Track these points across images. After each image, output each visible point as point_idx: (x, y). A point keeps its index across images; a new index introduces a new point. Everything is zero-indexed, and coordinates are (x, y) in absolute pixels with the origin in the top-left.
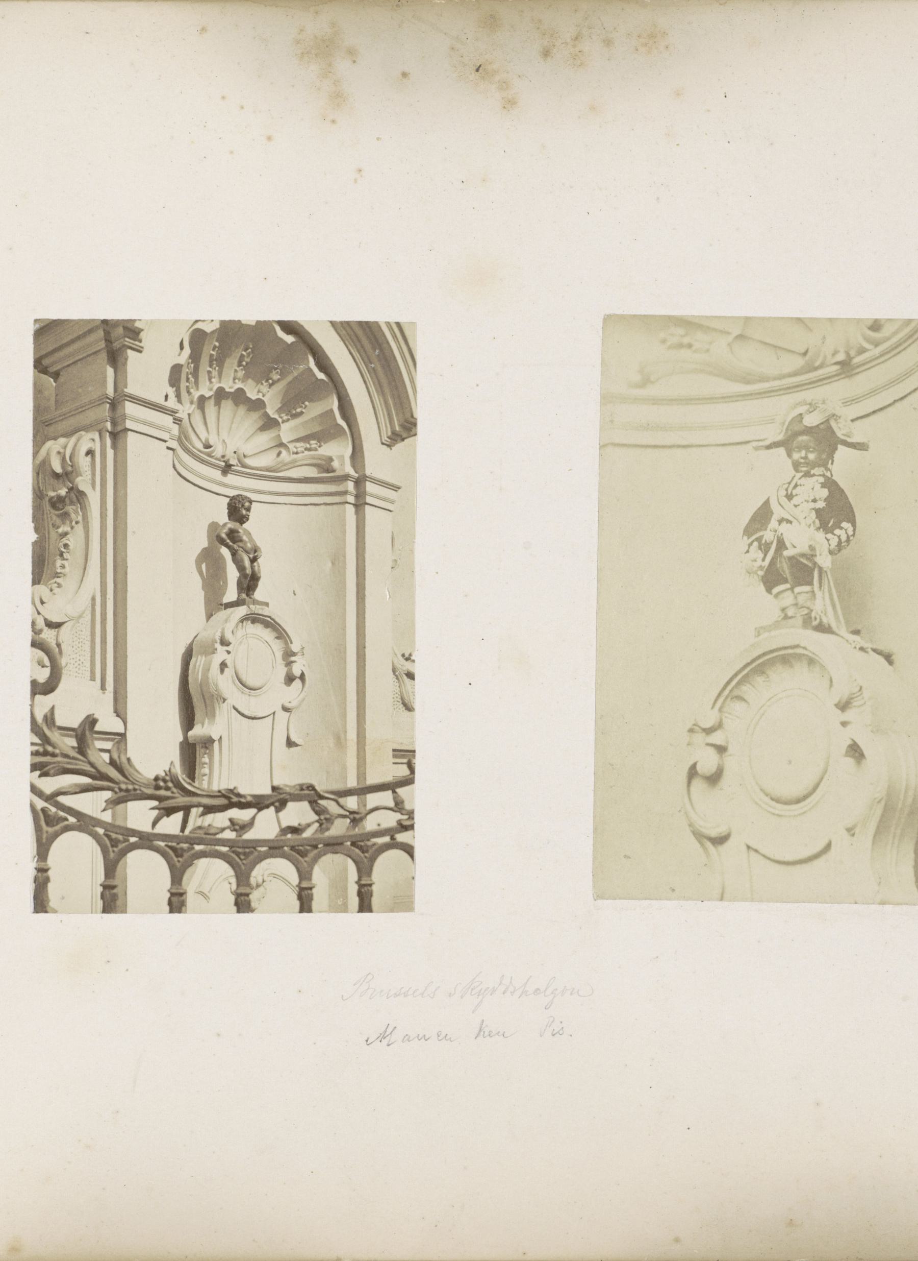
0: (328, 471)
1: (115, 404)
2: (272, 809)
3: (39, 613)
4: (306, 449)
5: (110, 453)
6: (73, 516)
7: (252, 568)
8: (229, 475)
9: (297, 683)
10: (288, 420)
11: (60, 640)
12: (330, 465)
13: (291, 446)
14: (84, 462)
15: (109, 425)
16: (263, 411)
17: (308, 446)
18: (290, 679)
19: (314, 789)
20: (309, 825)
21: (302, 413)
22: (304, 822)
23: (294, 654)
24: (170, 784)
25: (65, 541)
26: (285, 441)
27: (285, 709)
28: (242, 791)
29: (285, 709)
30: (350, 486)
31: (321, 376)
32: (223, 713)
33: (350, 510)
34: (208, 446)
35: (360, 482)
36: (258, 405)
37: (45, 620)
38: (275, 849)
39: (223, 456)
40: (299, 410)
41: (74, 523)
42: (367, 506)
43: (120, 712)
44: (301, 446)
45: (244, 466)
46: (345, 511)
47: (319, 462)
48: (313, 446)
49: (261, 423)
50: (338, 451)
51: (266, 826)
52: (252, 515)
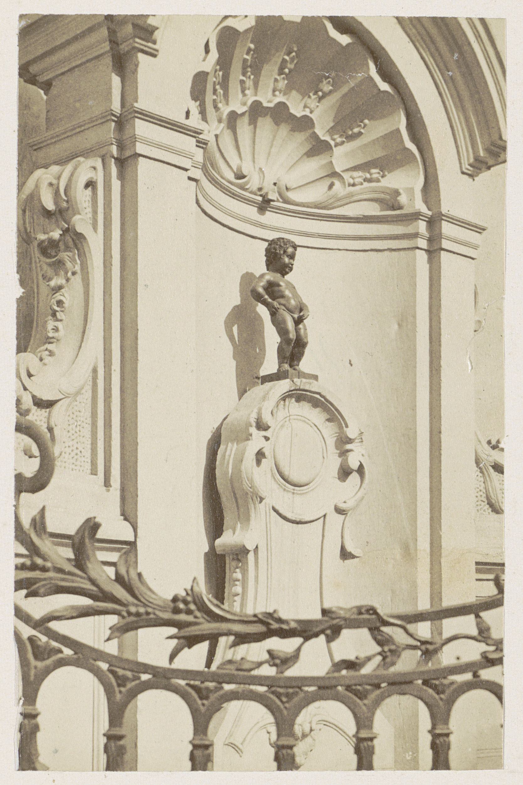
0: (393, 208)
1: (121, 123)
2: (322, 637)
3: (25, 389)
4: (365, 180)
5: (116, 185)
6: (69, 265)
7: (297, 331)
8: (267, 213)
9: (355, 477)
10: (343, 143)
11: (52, 424)
12: (396, 200)
13: (346, 176)
14: (82, 197)
15: (114, 150)
16: (310, 131)
18: (345, 473)
19: (375, 612)
20: (369, 659)
21: (360, 134)
22: (363, 655)
23: (350, 441)
24: (192, 607)
25: (58, 296)
26: (338, 170)
27: (339, 511)
28: (284, 615)
29: (339, 511)
30: (422, 226)
31: (384, 86)
32: (260, 516)
33: (422, 257)
34: (240, 176)
35: (433, 222)
36: (304, 124)
37: (34, 397)
38: (325, 689)
39: (260, 189)
40: (356, 130)
41: (69, 274)
42: (442, 252)
43: (128, 514)
44: (359, 175)
45: (286, 201)
46: (415, 259)
47: (382, 196)
48: (375, 176)
50: (406, 182)
51: (314, 659)
52: (296, 263)
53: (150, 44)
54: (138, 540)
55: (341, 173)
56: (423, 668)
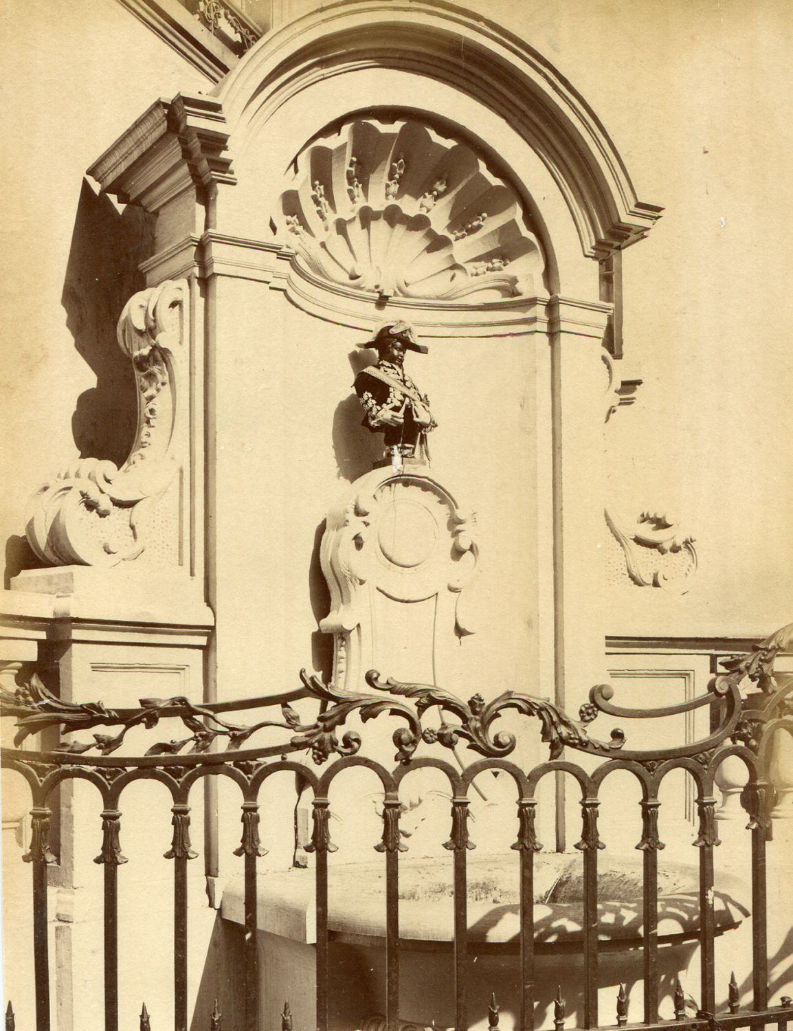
1: (202, 247)
2: (142, 725)
3: (102, 492)
5: (200, 302)
6: (159, 376)
8: (386, 307)
9: (468, 556)
10: (463, 236)
11: (134, 523)
14: (168, 317)
15: (196, 271)
16: (427, 229)
17: (490, 265)
18: (457, 553)
19: (187, 703)
20: (184, 743)
21: (479, 227)
22: (178, 740)
23: (461, 522)
24: (31, 699)
25: (151, 405)
26: (459, 261)
27: (452, 590)
28: (106, 706)
30: (540, 311)
31: (496, 182)
32: (359, 595)
34: (354, 277)
35: (552, 307)
36: (419, 223)
37: (112, 500)
38: (145, 768)
39: (377, 287)
40: (475, 223)
41: (159, 385)
42: (562, 334)
44: (482, 266)
45: (406, 295)
47: (503, 283)
49: (426, 243)
51: (137, 743)
53: (227, 175)
54: (217, 624)
55: (464, 265)
56: (234, 750)
